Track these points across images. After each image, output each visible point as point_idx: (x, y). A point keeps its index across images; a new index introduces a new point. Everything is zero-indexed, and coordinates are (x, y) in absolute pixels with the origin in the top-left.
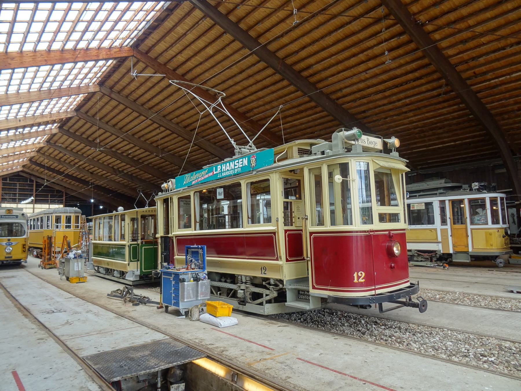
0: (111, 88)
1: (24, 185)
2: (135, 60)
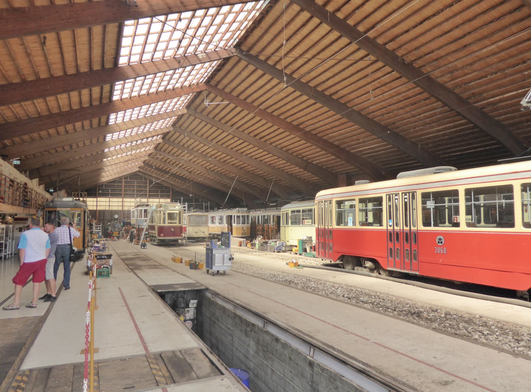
2: (207, 92)
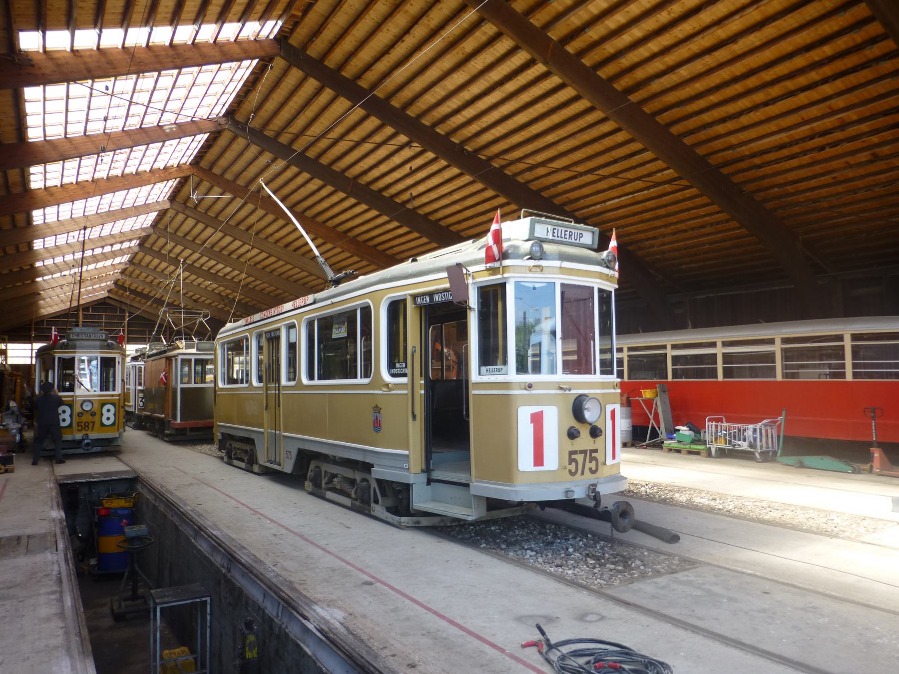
1: (113, 317)
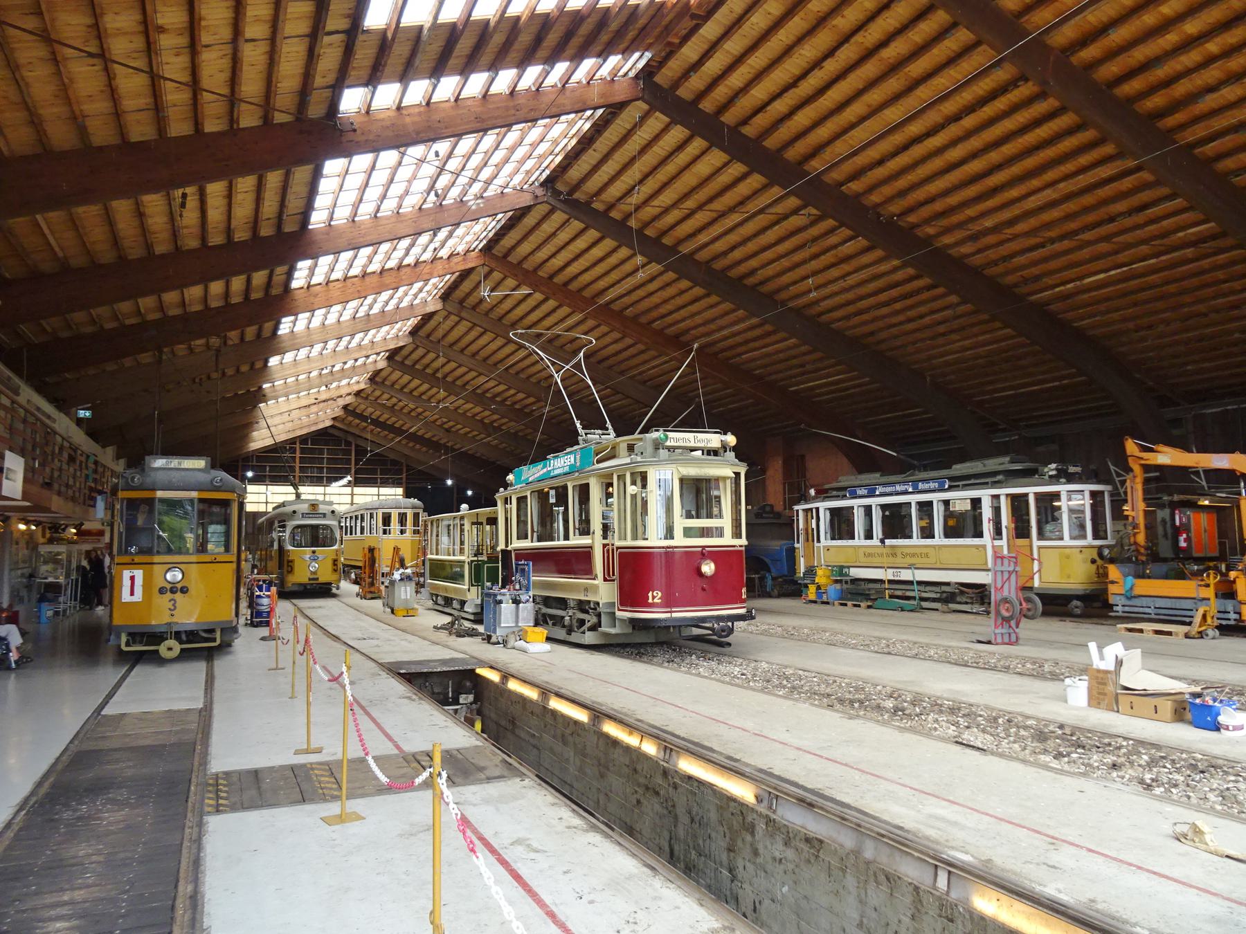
0: (461, 302)
